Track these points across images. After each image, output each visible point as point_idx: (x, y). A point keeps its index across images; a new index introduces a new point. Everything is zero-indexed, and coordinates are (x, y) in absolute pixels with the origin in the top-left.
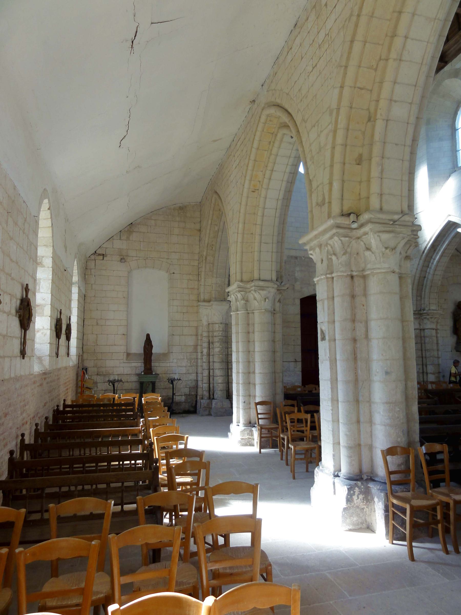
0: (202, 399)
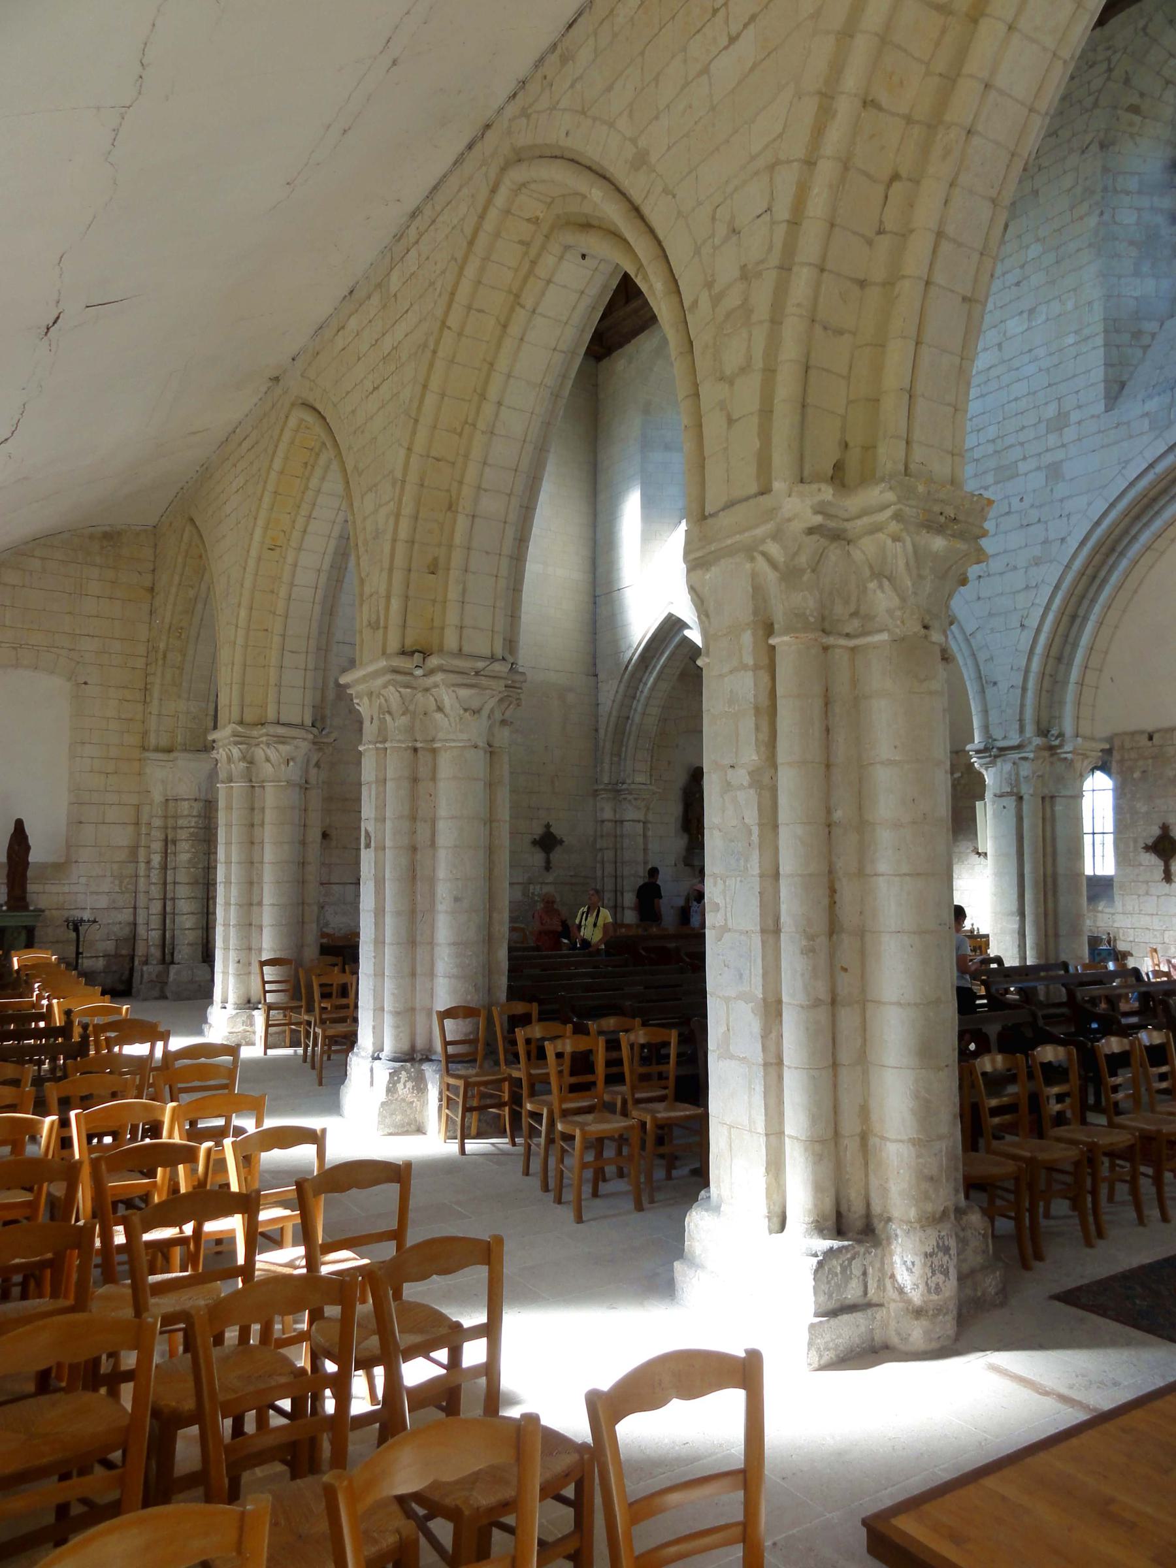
0: (146, 963)
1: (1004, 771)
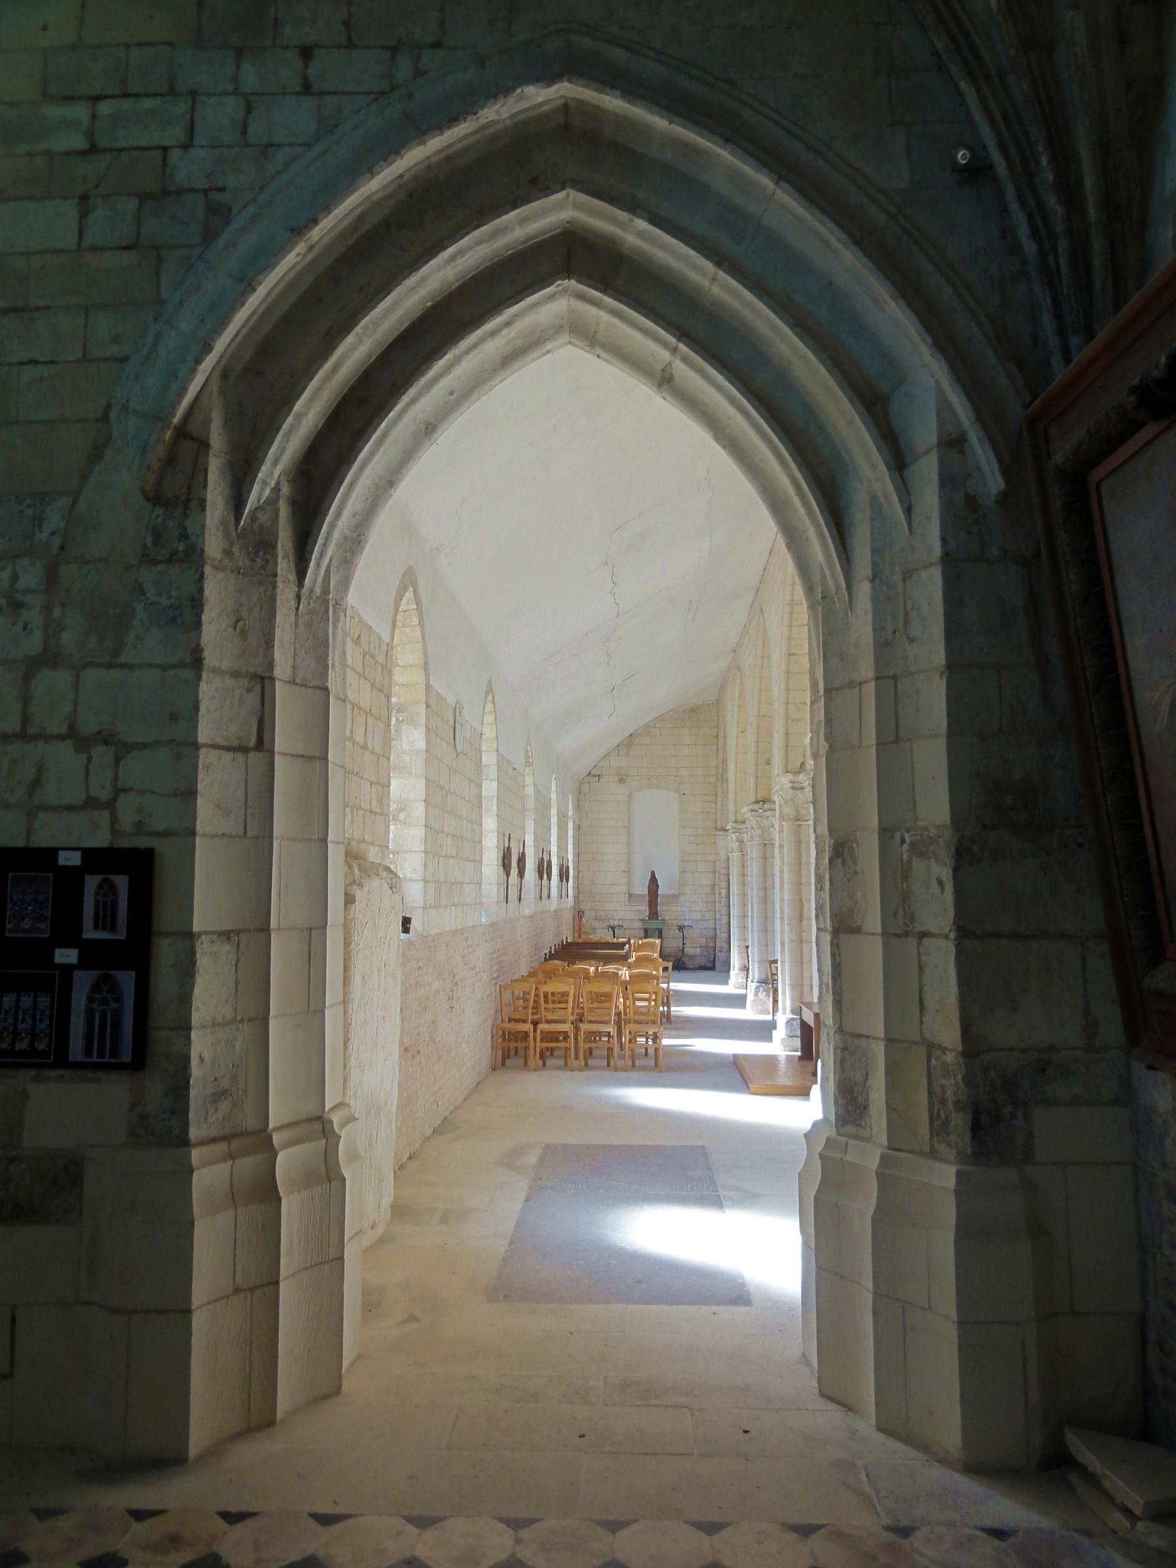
0: (720, 951)
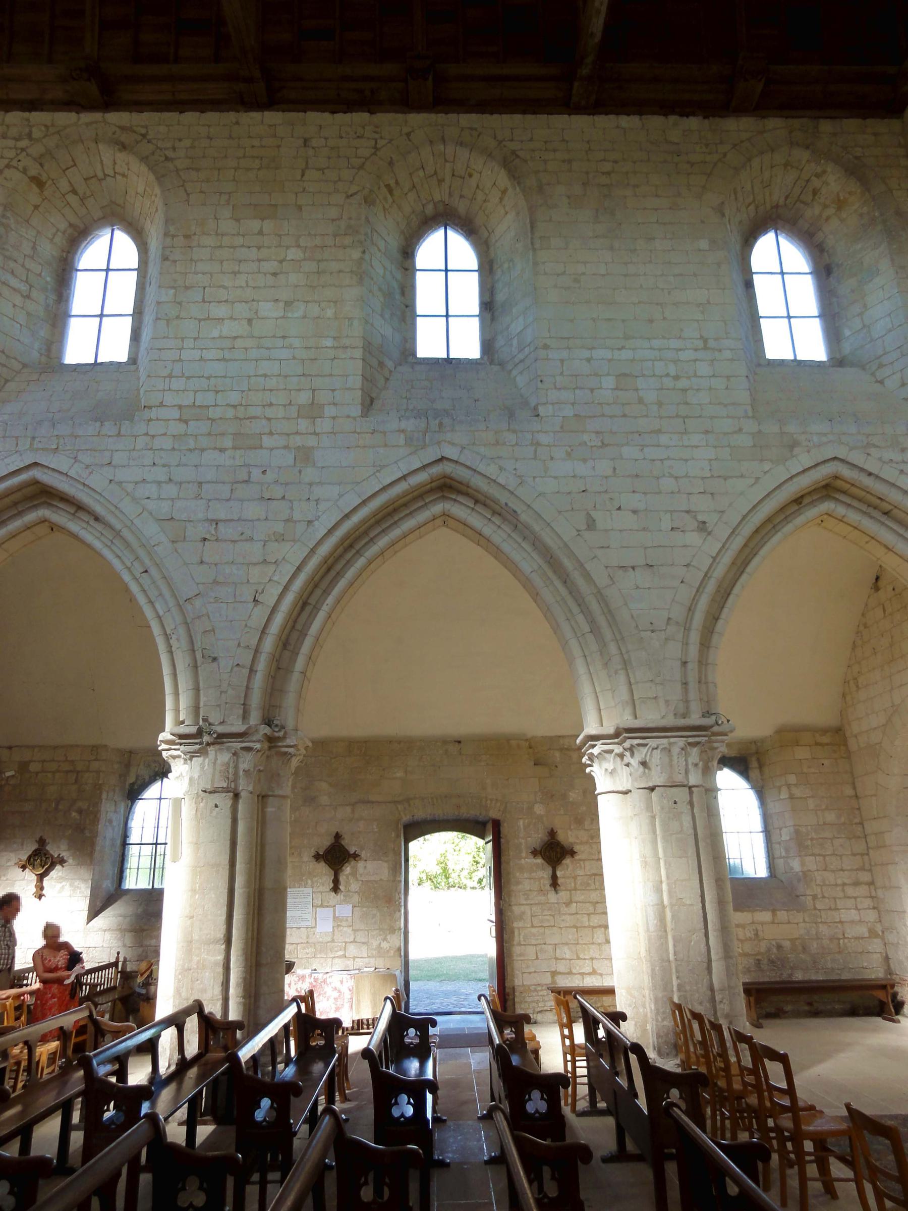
1: (219, 762)
